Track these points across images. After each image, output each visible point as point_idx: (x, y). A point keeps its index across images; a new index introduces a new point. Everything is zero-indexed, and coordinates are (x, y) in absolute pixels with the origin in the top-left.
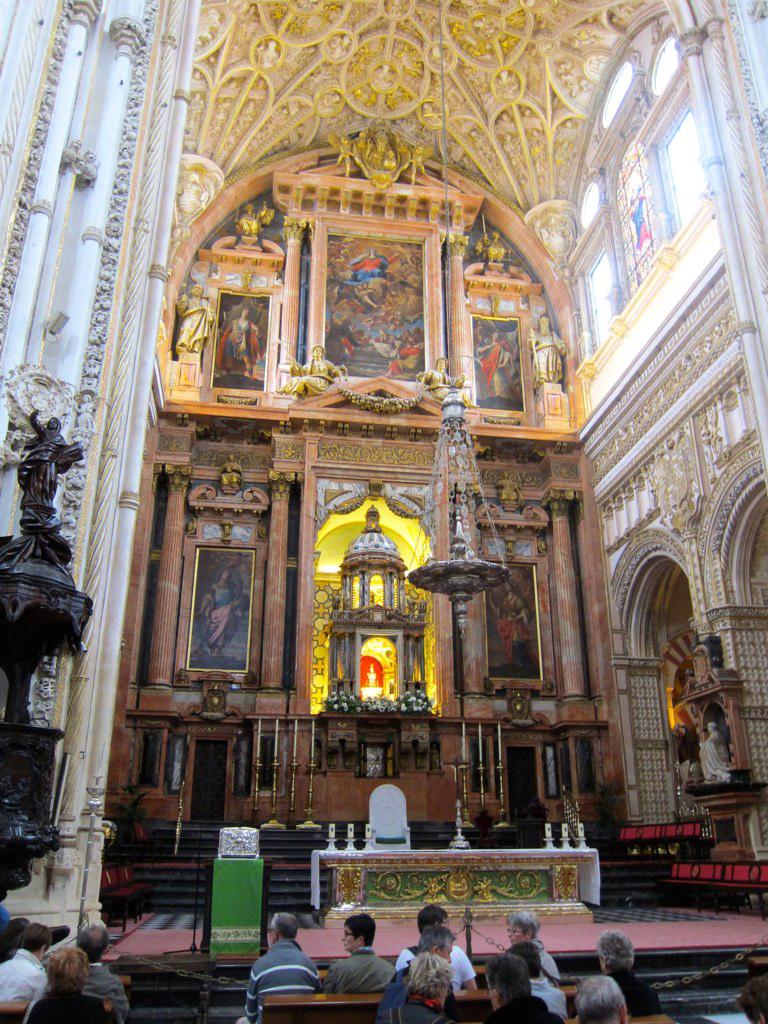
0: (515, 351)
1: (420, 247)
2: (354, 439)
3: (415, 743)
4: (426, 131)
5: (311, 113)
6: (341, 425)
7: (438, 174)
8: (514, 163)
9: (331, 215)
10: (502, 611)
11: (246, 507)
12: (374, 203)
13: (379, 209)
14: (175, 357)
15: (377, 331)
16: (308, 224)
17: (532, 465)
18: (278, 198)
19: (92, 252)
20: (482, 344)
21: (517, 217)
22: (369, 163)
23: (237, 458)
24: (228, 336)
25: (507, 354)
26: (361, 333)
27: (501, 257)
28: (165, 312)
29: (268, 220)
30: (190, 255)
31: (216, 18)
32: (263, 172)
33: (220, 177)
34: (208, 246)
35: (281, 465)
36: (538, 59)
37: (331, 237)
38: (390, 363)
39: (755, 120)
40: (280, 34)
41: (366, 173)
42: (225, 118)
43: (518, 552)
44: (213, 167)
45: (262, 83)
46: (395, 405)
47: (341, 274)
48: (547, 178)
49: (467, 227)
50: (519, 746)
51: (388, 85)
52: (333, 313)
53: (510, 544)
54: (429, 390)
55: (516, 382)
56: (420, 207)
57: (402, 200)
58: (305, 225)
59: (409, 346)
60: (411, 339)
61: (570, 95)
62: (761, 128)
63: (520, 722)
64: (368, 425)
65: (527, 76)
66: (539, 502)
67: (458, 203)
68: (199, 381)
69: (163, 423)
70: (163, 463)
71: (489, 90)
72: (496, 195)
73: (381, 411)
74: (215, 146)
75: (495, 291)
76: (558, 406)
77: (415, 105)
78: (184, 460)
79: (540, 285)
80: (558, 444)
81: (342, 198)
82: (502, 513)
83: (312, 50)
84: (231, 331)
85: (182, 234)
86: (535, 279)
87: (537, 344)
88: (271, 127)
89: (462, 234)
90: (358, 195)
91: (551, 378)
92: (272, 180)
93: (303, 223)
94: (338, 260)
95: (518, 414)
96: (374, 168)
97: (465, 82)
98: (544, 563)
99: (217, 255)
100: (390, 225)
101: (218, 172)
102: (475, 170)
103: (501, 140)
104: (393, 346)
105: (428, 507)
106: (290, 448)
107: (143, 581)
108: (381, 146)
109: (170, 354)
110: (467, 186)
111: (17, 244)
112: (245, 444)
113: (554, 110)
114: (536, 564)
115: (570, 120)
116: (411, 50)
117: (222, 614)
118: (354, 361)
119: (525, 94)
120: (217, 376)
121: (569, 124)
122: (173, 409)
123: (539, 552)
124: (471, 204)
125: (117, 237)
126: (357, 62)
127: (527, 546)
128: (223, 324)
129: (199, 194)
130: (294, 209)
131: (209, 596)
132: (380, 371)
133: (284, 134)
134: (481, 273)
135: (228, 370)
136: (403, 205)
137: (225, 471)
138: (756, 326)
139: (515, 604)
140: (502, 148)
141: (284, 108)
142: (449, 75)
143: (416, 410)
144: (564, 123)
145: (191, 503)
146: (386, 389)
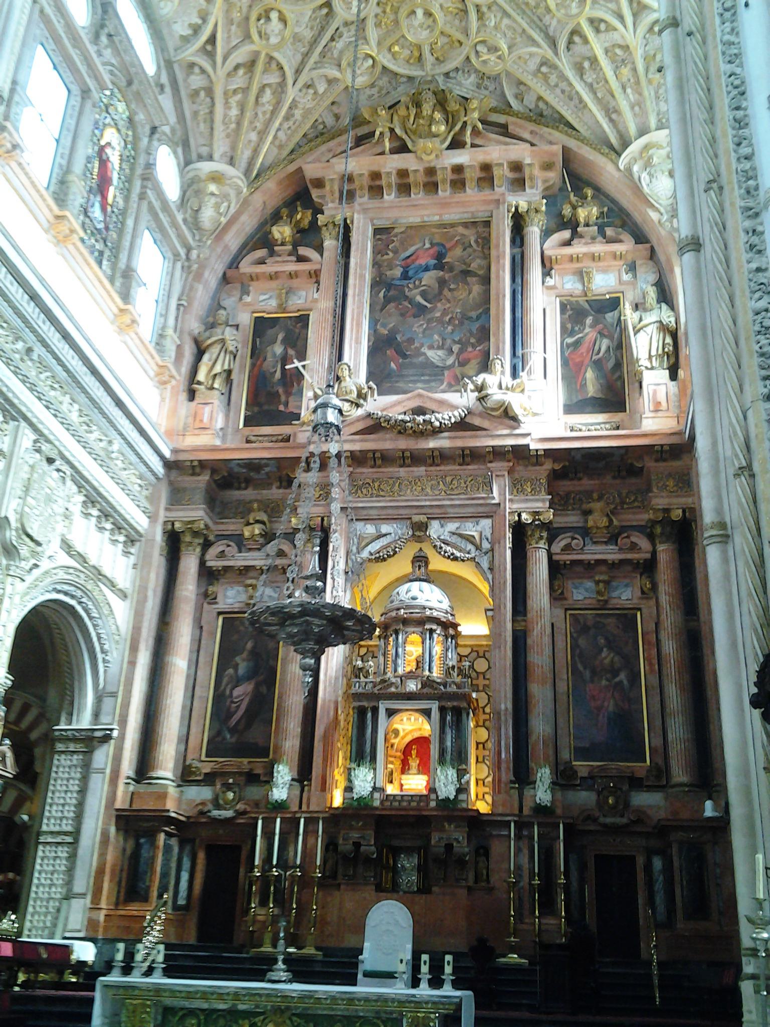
0: (616, 336)
1: (487, 224)
2: (391, 469)
3: (449, 847)
4: (489, 78)
5: (342, 87)
6: (371, 455)
7: (504, 130)
9: (375, 203)
10: (594, 672)
12: (426, 180)
13: (432, 187)
14: (192, 395)
15: (431, 336)
16: (345, 220)
17: (633, 480)
18: (315, 193)
20: (572, 333)
22: (414, 133)
24: (261, 365)
28: (179, 347)
29: (305, 223)
30: (212, 278)
32: (292, 168)
33: (242, 184)
34: (234, 263)
37: (377, 231)
38: (446, 373)
43: (615, 594)
44: (234, 173)
46: (431, 423)
47: (388, 273)
49: (546, 189)
50: (612, 853)
53: (601, 585)
55: (617, 374)
56: (483, 175)
57: (458, 169)
59: (470, 349)
60: (473, 340)
63: (609, 820)
64: (403, 451)
66: (640, 529)
67: (528, 161)
68: (220, 422)
69: (174, 473)
72: (583, 140)
73: (414, 432)
74: (234, 147)
76: (662, 397)
77: (466, 50)
82: (590, 547)
83: (325, 11)
84: (265, 359)
85: (198, 256)
86: (640, 237)
87: (641, 320)
88: (298, 113)
89: (538, 198)
90: (403, 174)
93: (339, 219)
94: (386, 257)
95: (618, 417)
98: (648, 607)
99: (244, 274)
100: (446, 203)
101: (239, 178)
102: (556, 115)
104: (451, 351)
105: (486, 545)
106: (318, 489)
107: (144, 659)
108: (427, 109)
109: (183, 396)
114: (640, 609)
117: (243, 692)
118: (403, 376)
120: (249, 413)
122: (182, 457)
123: (643, 592)
126: (384, 12)
127: (627, 586)
128: (255, 353)
129: (217, 206)
130: (330, 205)
131: (231, 671)
132: (433, 384)
133: (316, 116)
134: (568, 243)
135: (259, 405)
137: (248, 524)
139: (612, 661)
143: (462, 425)
145: (209, 564)
146: (425, 405)
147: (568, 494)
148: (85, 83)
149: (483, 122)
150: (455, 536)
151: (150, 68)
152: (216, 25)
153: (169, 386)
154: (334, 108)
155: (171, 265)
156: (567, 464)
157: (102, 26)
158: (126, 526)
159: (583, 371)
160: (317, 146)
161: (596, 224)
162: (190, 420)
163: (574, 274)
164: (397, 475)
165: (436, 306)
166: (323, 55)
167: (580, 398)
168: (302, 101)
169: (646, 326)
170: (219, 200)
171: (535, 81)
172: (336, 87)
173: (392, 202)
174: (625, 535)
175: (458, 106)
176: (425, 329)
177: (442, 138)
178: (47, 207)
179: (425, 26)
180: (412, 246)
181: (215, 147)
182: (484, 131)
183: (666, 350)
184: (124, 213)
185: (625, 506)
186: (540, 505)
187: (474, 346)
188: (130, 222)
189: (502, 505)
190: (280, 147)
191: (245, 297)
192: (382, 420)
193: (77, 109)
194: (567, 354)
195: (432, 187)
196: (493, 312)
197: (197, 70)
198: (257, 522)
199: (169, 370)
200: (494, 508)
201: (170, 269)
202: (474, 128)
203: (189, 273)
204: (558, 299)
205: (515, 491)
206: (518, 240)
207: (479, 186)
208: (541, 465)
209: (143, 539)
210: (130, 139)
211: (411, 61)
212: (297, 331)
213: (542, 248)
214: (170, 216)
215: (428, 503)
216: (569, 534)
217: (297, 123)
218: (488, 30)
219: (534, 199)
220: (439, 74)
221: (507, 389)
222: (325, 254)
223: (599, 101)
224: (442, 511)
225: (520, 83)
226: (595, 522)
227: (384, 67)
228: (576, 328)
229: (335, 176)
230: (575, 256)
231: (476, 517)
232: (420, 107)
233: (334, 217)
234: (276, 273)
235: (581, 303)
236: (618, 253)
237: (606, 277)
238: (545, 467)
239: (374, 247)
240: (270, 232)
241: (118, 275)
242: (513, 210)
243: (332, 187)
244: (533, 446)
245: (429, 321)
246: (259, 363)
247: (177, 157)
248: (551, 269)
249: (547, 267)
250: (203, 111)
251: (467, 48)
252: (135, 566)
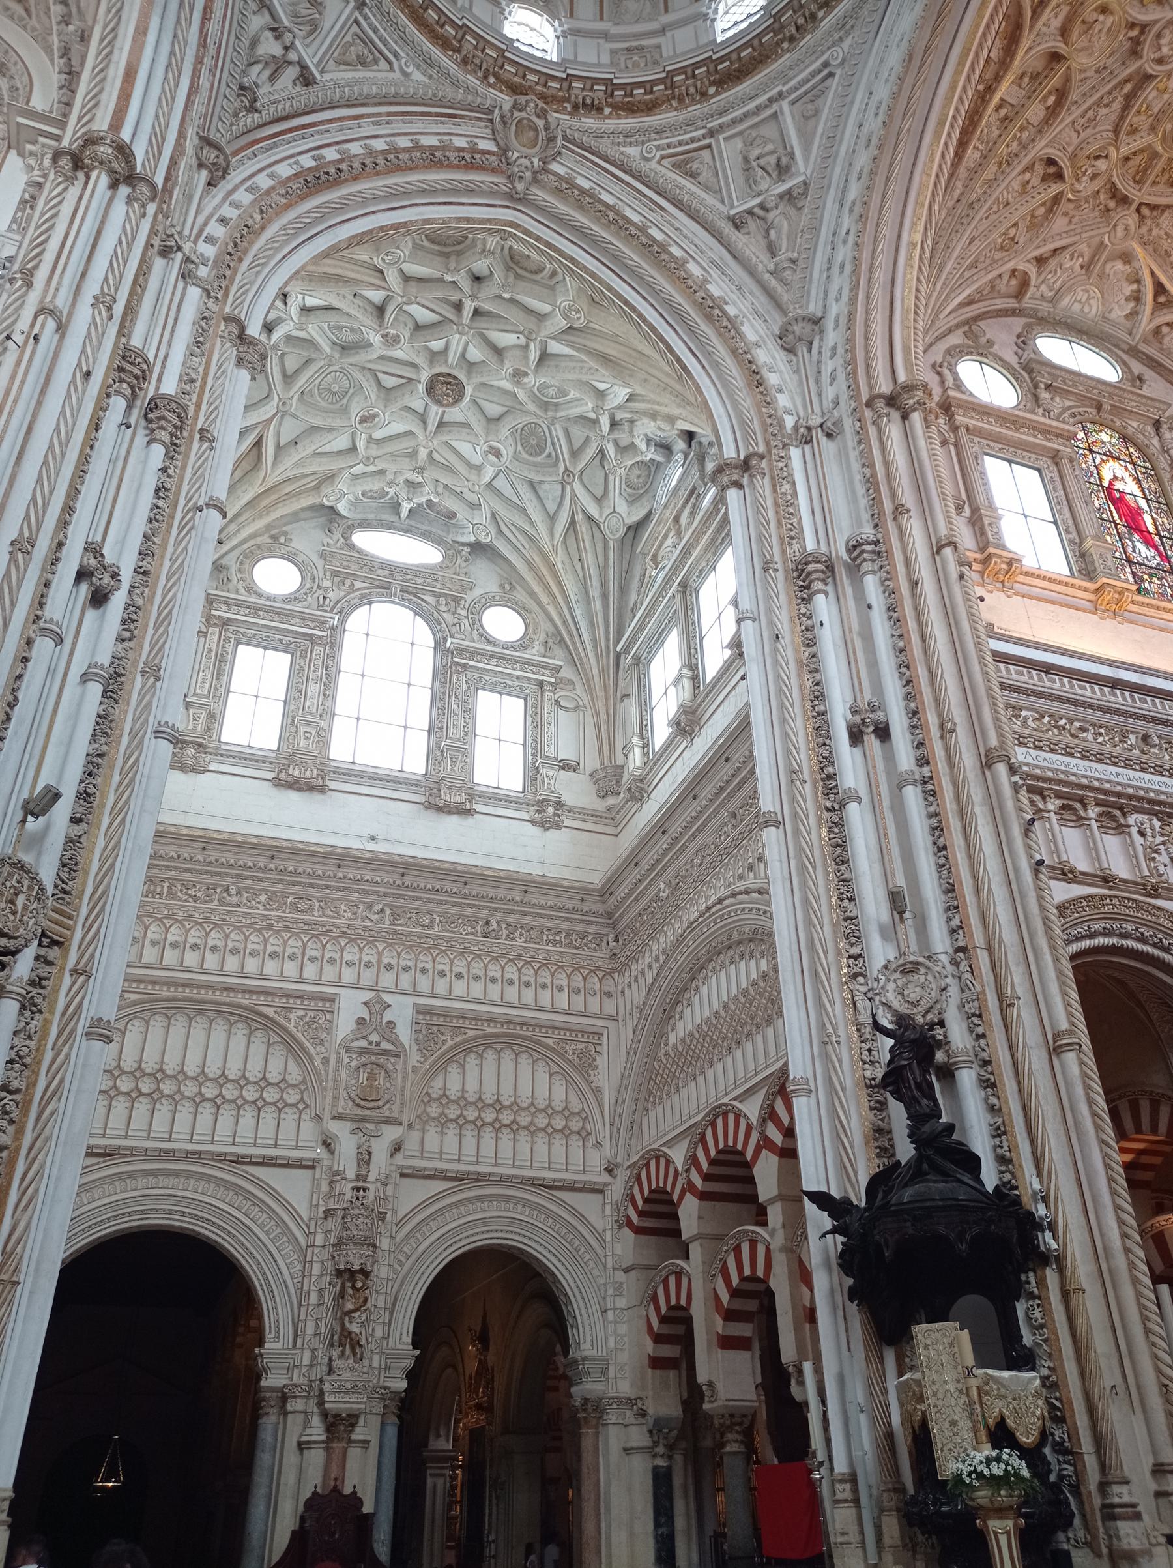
19: (912, 796)
31: (1119, 266)
111: (839, 851)
125: (928, 763)
148: (1049, 448)
152: (1152, 273)
157: (1036, 387)
193: (1057, 478)
197: (1165, 330)
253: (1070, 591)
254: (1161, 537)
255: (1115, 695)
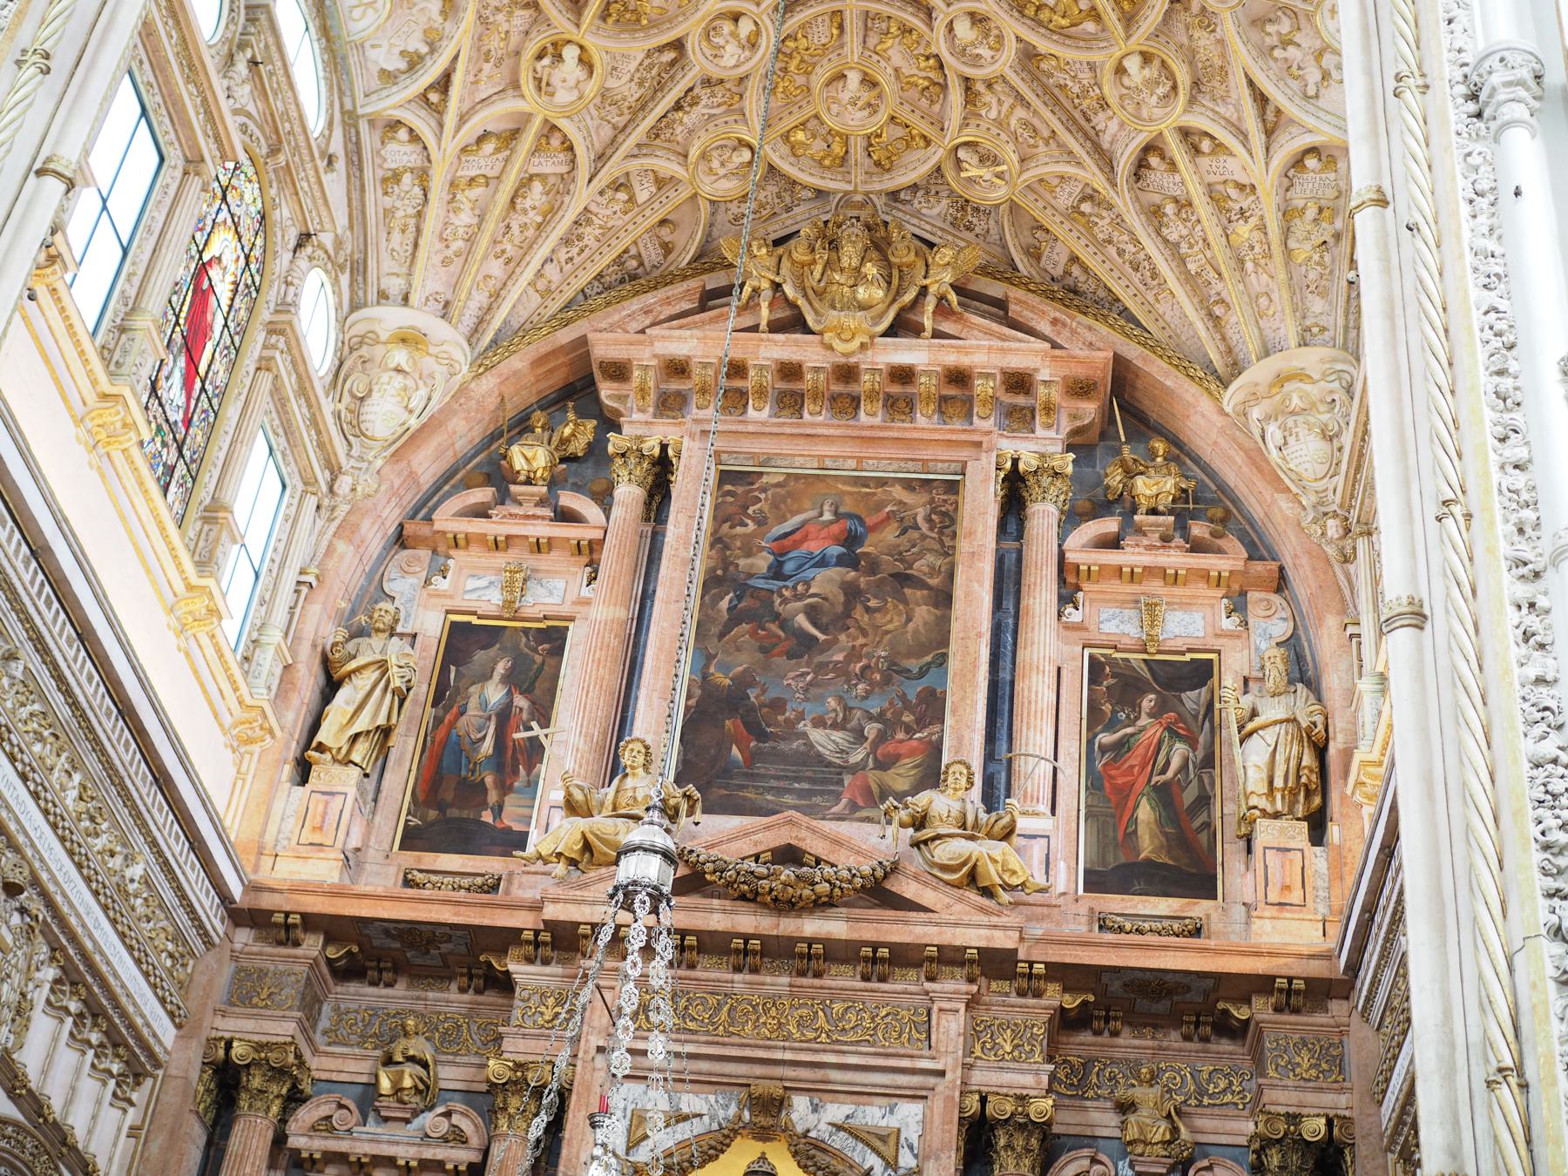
0: (1201, 739)
1: (953, 487)
2: (713, 975)
4: (977, 210)
5: (685, 193)
7: (999, 309)
8: (1192, 267)
11: (429, 1153)
13: (847, 405)
14: (303, 771)
15: (821, 699)
16: (664, 447)
17: (1226, 1046)
18: (607, 391)
20: (1111, 726)
21: (1206, 395)
22: (820, 294)
23: (429, 1027)
24: (452, 724)
25: (1180, 749)
26: (778, 705)
27: (1165, 502)
28: (287, 667)
29: (578, 446)
30: (375, 536)
32: (566, 336)
33: (462, 356)
34: (424, 508)
35: (522, 1045)
36: (1207, 20)
37: (725, 477)
38: (847, 779)
39: (1462, 89)
40: (584, 27)
41: (810, 319)
42: (475, 221)
45: (556, 142)
46: (813, 884)
47: (743, 562)
48: (1275, 296)
49: (1076, 432)
51: (866, 113)
52: (710, 658)
54: (916, 844)
57: (903, 375)
58: (657, 451)
59: (901, 735)
61: (1306, 97)
62: (1472, 107)
64: (747, 938)
65: (1191, 56)
67: (1044, 375)
69: (243, 936)
70: (227, 1035)
71: (1104, 104)
72: (1154, 347)
73: (776, 900)
74: (455, 287)
75: (1155, 586)
77: (937, 154)
78: (282, 1028)
79: (1274, 566)
80: (1281, 983)
81: (749, 384)
83: (669, 56)
84: (462, 713)
85: (353, 490)
86: (1257, 548)
88: (590, 233)
89: (1059, 448)
90: (790, 371)
91: (1279, 806)
92: (588, 353)
93: (652, 447)
94: (739, 530)
95: (1199, 908)
96: (834, 308)
97: (1044, 86)
99: (444, 533)
100: (872, 439)
102: (1101, 293)
103: (1154, 214)
106: (551, 1001)
108: (849, 254)
109: (288, 770)
110: (1073, 332)
112: (453, 994)
113: (1269, 133)
115: (1313, 150)
116: (906, 30)
118: (752, 776)
119: (1192, 100)
120: (415, 821)
121: (1311, 162)
122: (266, 901)
124: (1080, 372)
126: (785, 70)
130: (636, 416)
132: (817, 800)
135: (441, 807)
136: (909, 389)
137: (388, 1061)
138: (1427, 611)
140: (1159, 234)
141: (617, 186)
142: (1003, 77)
144: (1298, 163)
145: (295, 1142)
146: (802, 845)
147: (1087, 1064)
148: (195, 146)
149: (958, 289)
150: (842, 1134)
151: (316, 122)
152: (456, 58)
153: (256, 748)
154: (665, 232)
155: (295, 502)
156: (1091, 998)
157: (242, 46)
158: (131, 1042)
159: (1130, 804)
160: (624, 298)
161: (1171, 512)
162: (292, 824)
163: (1123, 604)
164: (727, 988)
165: (836, 641)
166: (655, 132)
167: (1123, 860)
168: (603, 212)
169: (1263, 727)
170: (410, 382)
171: (1067, 225)
172: (672, 194)
173: (763, 424)
174: (1205, 1163)
175: (912, 257)
176: (810, 684)
177: (874, 312)
178: (88, 375)
179: (860, 104)
180: (794, 513)
181: (417, 281)
182: (959, 309)
183: (1304, 780)
184: (222, 394)
185: (1206, 1101)
186: (1028, 1080)
187: (909, 730)
188: (232, 412)
189: (949, 1076)
190: (547, 293)
191: (437, 579)
192: (709, 867)
193: (172, 192)
194: (1099, 765)
195: (847, 405)
196: (953, 664)
197: (403, 134)
198: (411, 1059)
199: (265, 717)
200: (931, 1081)
201: (293, 509)
202: (942, 298)
203: (331, 520)
204: (1087, 652)
205: (978, 1047)
206: (1012, 527)
207: (941, 412)
208: (1038, 994)
209: (160, 1072)
210: (257, 252)
211: (827, 162)
212: (538, 659)
213: (1060, 546)
214: (310, 406)
215: (788, 1056)
216: (1086, 1152)
217: (587, 252)
218: (984, 125)
219: (1051, 449)
220: (879, 193)
221: (976, 826)
222: (616, 512)
223: (1190, 279)
224: (819, 1074)
225: (1041, 227)
226: (1141, 1131)
227: (771, 168)
228: (1122, 716)
229: (654, 363)
230: (1126, 570)
231: (893, 1095)
232: (837, 249)
233: (640, 439)
234: (508, 537)
235: (1134, 664)
236: (1214, 574)
237: (1186, 616)
238: (1043, 1002)
239: (717, 507)
240: (505, 457)
241: (194, 513)
242: (1008, 465)
243: (643, 381)
244: (1021, 955)
245: (821, 668)
246: (448, 717)
247: (337, 293)
248: (1079, 589)
249: (1069, 583)
250: (406, 209)
251: (941, 153)
252: (134, 1132)
253: (76, 365)
254: (203, 389)
255: (27, 565)
